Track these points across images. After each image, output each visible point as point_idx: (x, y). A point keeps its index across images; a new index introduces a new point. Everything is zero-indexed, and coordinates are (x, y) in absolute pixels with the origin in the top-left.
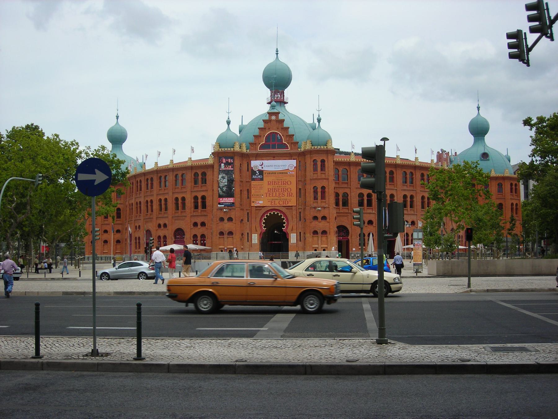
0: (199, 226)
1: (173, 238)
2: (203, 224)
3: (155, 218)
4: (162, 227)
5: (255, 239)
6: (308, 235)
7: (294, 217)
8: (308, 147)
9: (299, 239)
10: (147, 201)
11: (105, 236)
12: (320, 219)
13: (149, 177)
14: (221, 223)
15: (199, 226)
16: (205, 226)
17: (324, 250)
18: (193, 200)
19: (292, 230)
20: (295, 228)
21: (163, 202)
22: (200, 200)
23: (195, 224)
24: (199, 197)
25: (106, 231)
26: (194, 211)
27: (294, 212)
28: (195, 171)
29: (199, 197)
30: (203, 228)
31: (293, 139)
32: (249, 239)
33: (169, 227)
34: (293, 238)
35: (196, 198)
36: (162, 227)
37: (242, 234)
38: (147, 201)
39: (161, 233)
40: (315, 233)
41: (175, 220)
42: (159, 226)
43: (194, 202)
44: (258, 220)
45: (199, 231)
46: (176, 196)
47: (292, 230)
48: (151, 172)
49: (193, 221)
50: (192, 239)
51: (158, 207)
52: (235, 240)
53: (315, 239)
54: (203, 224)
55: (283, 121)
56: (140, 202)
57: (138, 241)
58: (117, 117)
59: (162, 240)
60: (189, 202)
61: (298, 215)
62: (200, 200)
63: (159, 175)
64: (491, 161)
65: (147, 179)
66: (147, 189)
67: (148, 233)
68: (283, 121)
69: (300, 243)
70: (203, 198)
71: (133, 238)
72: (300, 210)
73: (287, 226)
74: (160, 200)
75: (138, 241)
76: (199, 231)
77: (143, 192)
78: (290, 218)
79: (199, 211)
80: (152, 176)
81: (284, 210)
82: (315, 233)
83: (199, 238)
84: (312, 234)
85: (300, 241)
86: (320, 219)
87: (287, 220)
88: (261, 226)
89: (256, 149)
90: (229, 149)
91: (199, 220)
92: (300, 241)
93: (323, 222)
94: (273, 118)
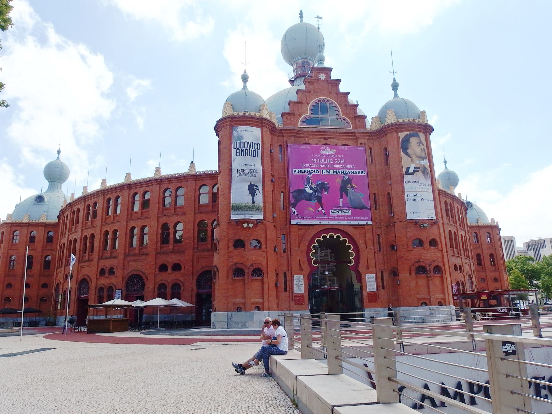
0: (170, 271)
2: (177, 267)
3: (96, 260)
4: (107, 274)
5: (299, 284)
6: (404, 275)
7: (370, 243)
8: (390, 119)
9: (381, 285)
10: (86, 236)
12: (427, 245)
13: (91, 202)
14: (238, 251)
15: (170, 271)
16: (180, 269)
17: (440, 304)
18: (160, 231)
19: (368, 267)
20: (372, 263)
21: (110, 236)
23: (163, 268)
26: (161, 248)
27: (369, 235)
28: (164, 186)
31: (356, 112)
32: (288, 286)
33: (119, 273)
34: (371, 284)
35: (165, 227)
36: (107, 274)
37: (277, 275)
38: (86, 236)
39: (105, 281)
40: (421, 270)
43: (162, 234)
44: (304, 248)
45: (170, 277)
46: (132, 224)
47: (368, 267)
48: (96, 194)
49: (160, 262)
50: (156, 290)
52: (266, 287)
53: (422, 281)
55: (337, 82)
56: (75, 239)
58: (59, 152)
59: (105, 294)
61: (376, 241)
63: (107, 197)
64: (474, 210)
65: (89, 206)
66: (88, 219)
68: (337, 82)
69: (382, 292)
71: (61, 292)
72: (378, 231)
73: (357, 259)
74: (107, 233)
76: (170, 277)
77: (80, 225)
78: (361, 245)
79: (171, 247)
80: (95, 200)
81: (351, 231)
82: (421, 270)
84: (414, 274)
85: (383, 288)
86: (427, 245)
87: (357, 249)
88: (309, 260)
89: (296, 124)
90: (252, 114)
91: (171, 260)
92: (383, 288)
93: (433, 249)
94: (322, 77)
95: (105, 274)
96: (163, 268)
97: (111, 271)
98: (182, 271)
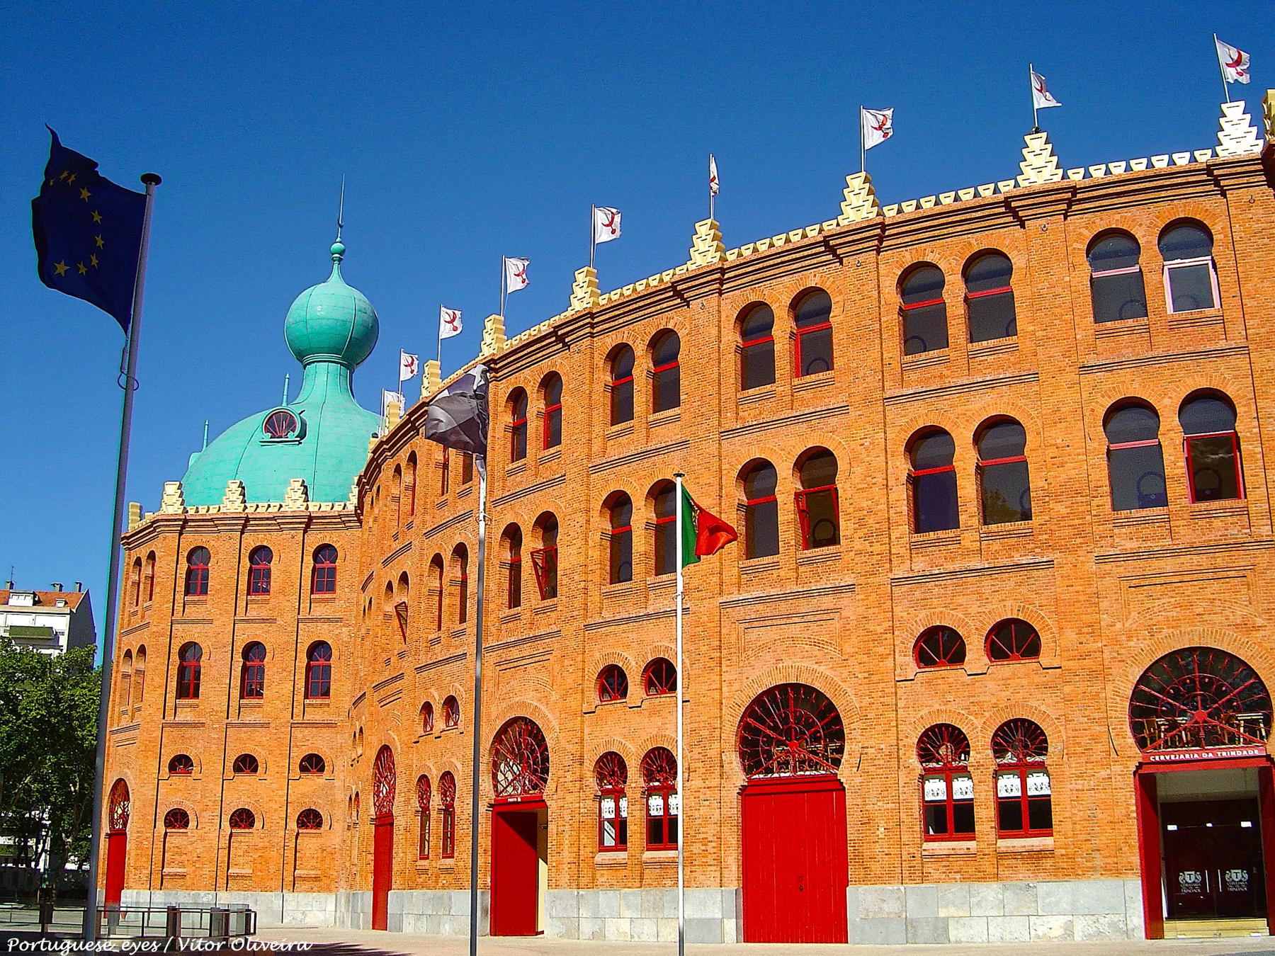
1: (733, 762)
2: (1013, 640)
11: (242, 792)
18: (902, 467)
22: (965, 460)
23: (939, 647)
24: (963, 437)
25: (247, 764)
26: (913, 547)
29: (963, 437)
30: (1017, 670)
36: (635, 689)
39: (630, 729)
41: (750, 623)
42: (612, 682)
51: (599, 554)
54: (1013, 640)
57: (436, 801)
60: (873, 485)
62: (965, 460)
63: (610, 341)
67: (524, 742)
70: (999, 432)
74: (618, 504)
75: (436, 801)
80: (546, 366)
83: (981, 753)
95: (624, 694)
96: (939, 647)
97: (661, 675)
98: (1045, 659)
